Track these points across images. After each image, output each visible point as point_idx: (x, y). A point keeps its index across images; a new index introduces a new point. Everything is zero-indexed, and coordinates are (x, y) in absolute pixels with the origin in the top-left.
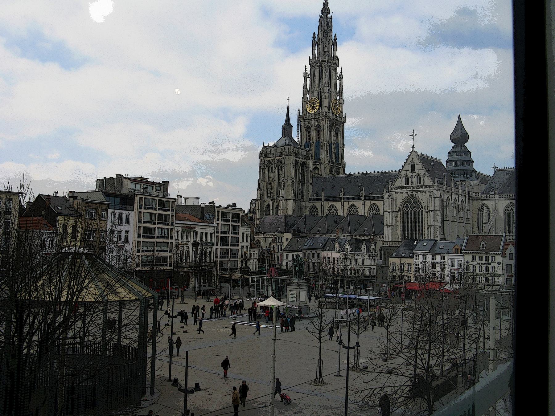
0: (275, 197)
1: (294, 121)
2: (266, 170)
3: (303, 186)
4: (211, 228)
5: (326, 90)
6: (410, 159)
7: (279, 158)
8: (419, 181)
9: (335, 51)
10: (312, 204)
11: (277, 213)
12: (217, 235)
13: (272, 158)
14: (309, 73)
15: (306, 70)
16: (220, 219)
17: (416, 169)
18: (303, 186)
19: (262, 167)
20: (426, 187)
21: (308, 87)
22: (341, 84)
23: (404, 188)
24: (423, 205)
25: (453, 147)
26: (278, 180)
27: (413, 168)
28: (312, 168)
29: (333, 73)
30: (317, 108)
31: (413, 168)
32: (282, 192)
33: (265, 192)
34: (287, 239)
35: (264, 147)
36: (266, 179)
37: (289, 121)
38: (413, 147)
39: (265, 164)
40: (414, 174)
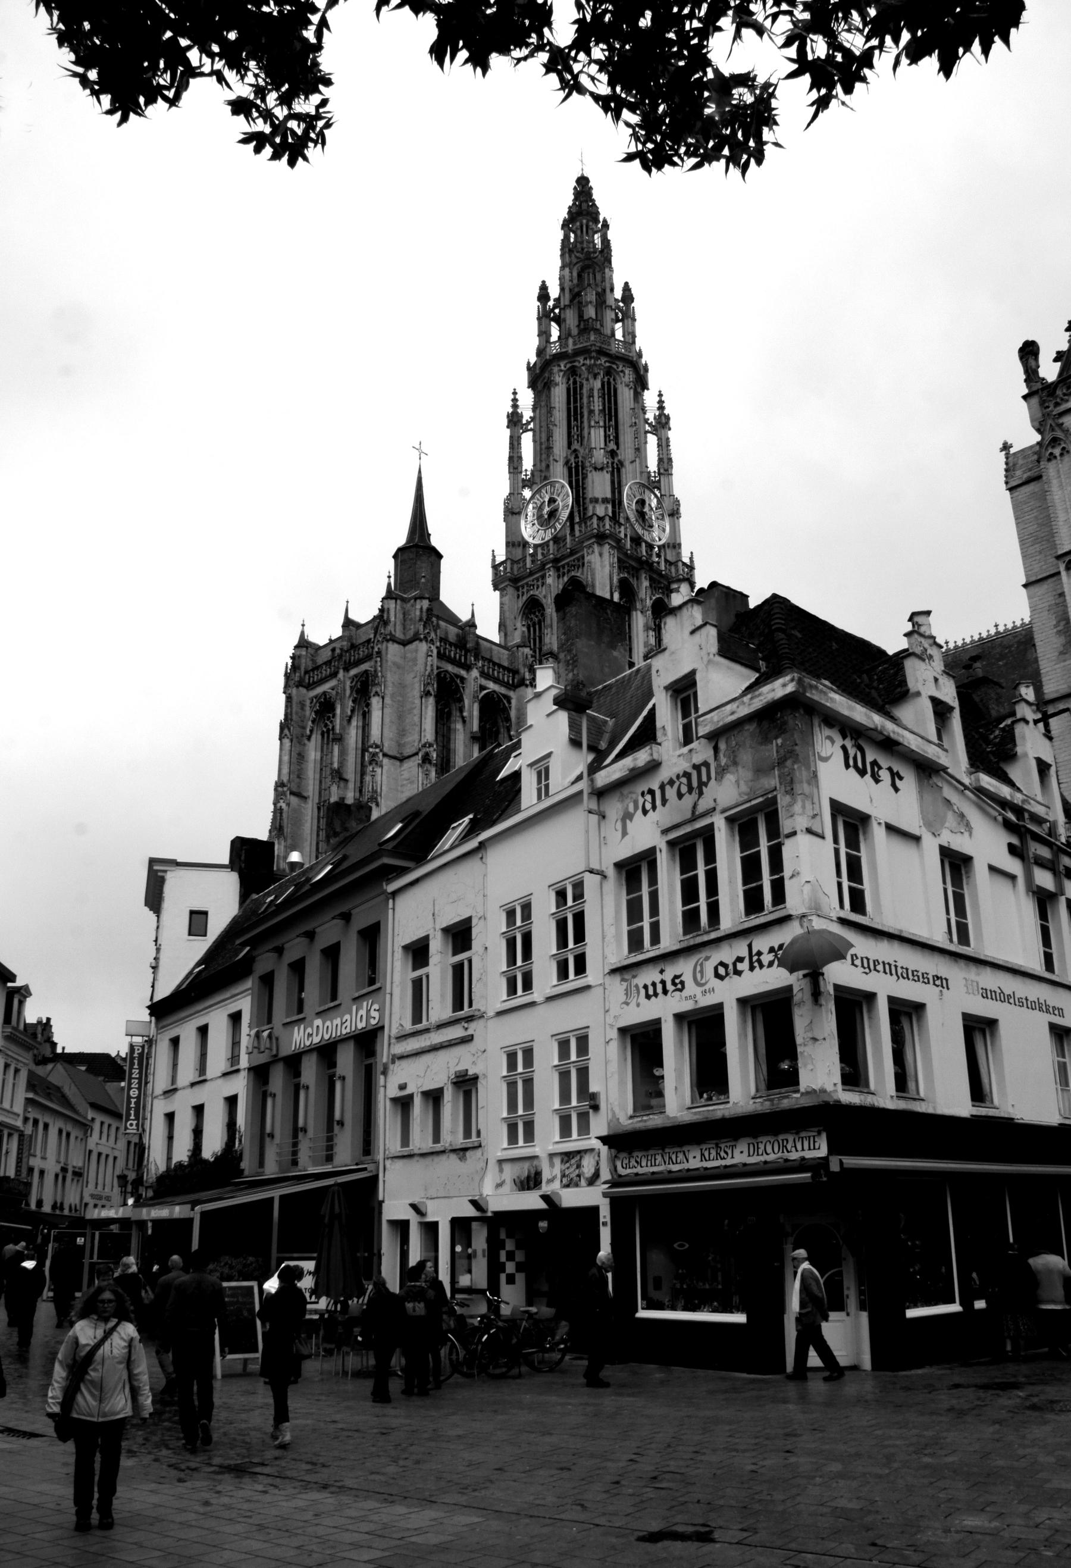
14: (527, 414)
15: (515, 406)
19: (290, 729)
21: (528, 463)
22: (664, 445)
34: (198, 920)
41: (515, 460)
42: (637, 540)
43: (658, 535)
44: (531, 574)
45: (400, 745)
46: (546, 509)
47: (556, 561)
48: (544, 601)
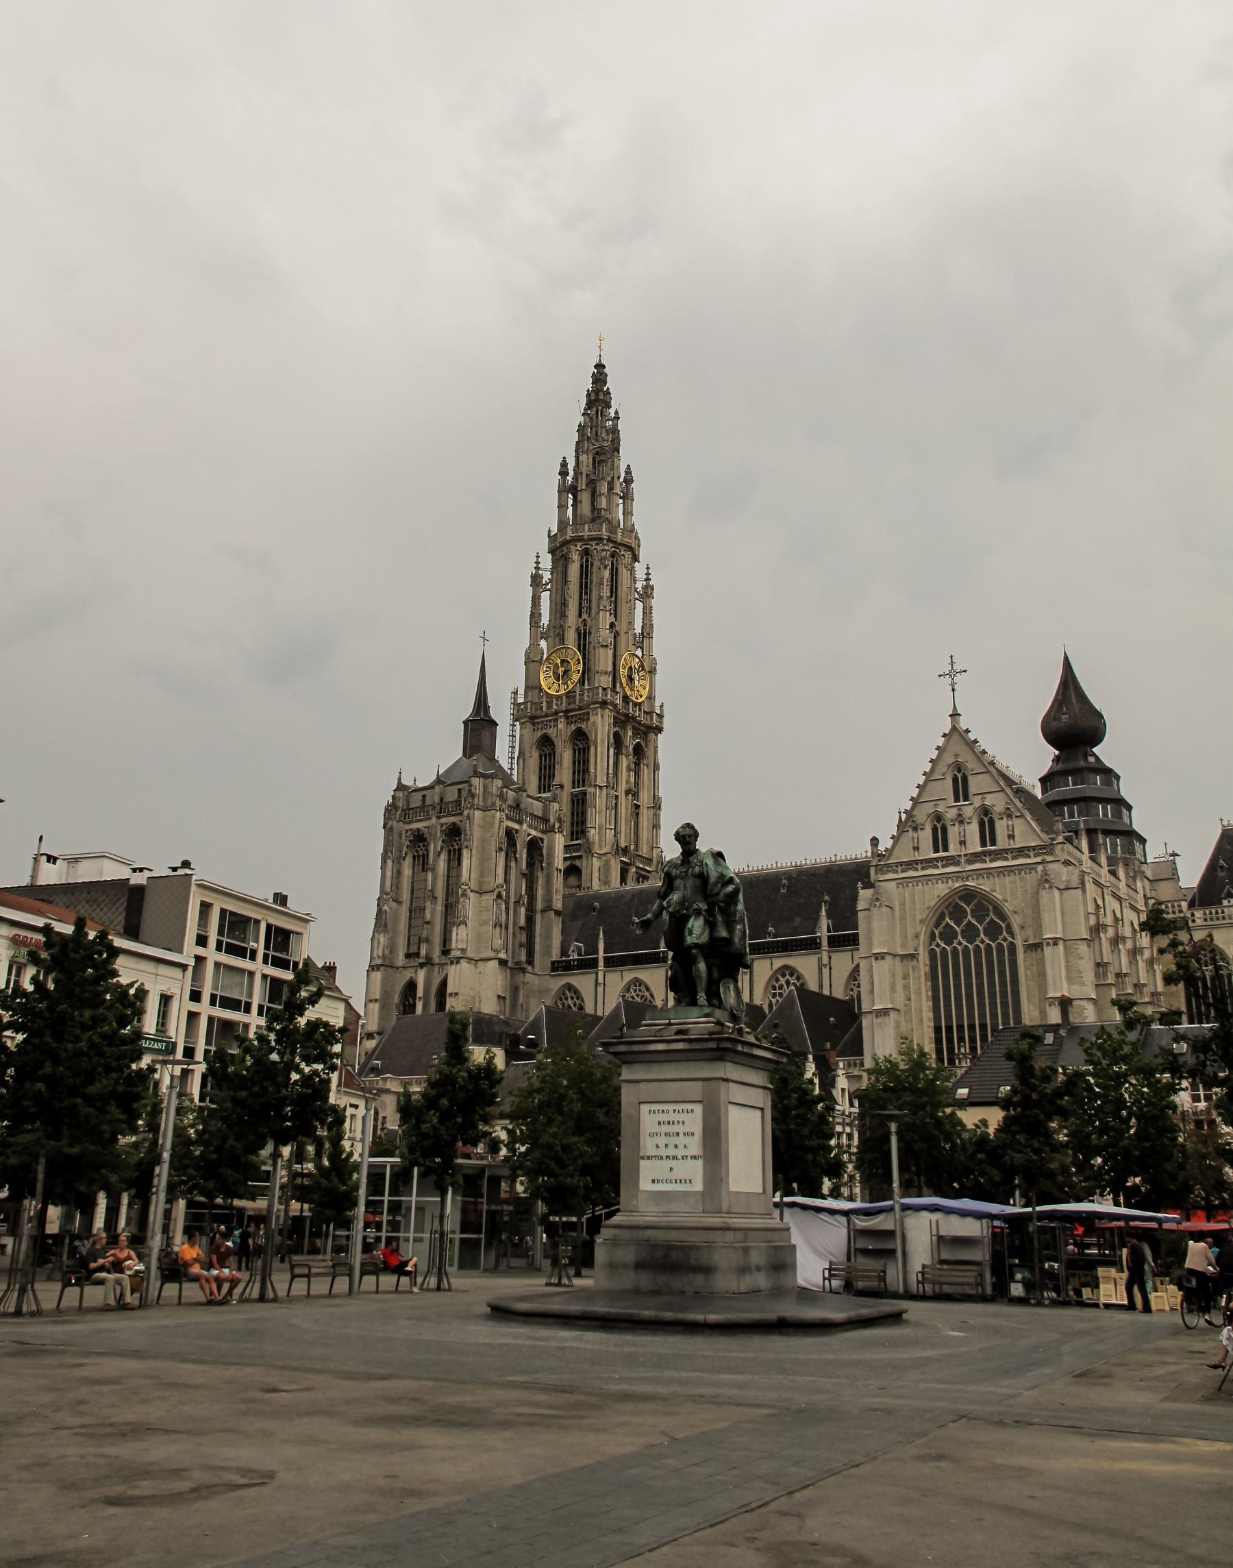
0: (436, 954)
1: (501, 711)
2: (408, 862)
3: (530, 919)
4: (163, 969)
5: (605, 619)
6: (949, 759)
7: (452, 819)
8: (988, 832)
9: (628, 513)
10: (562, 981)
11: (441, 1005)
12: (194, 1007)
13: (427, 823)
14: (547, 576)
15: (537, 568)
16: (212, 943)
17: (972, 789)
18: (530, 919)
19: (390, 851)
20: (1021, 852)
21: (545, 620)
22: (647, 612)
23: (928, 863)
24: (1015, 921)
25: (1057, 760)
26: (449, 892)
27: (961, 789)
28: (559, 862)
29: (624, 574)
30: (576, 677)
31: (961, 789)
32: (461, 937)
33: (402, 941)
35: (401, 787)
36: (405, 896)
37: (487, 708)
38: (955, 715)
39: (400, 846)
40: (968, 811)
41: (535, 616)
42: (626, 699)
43: (639, 692)
44: (546, 716)
45: (481, 883)
46: (561, 670)
47: (567, 711)
48: (555, 741)
